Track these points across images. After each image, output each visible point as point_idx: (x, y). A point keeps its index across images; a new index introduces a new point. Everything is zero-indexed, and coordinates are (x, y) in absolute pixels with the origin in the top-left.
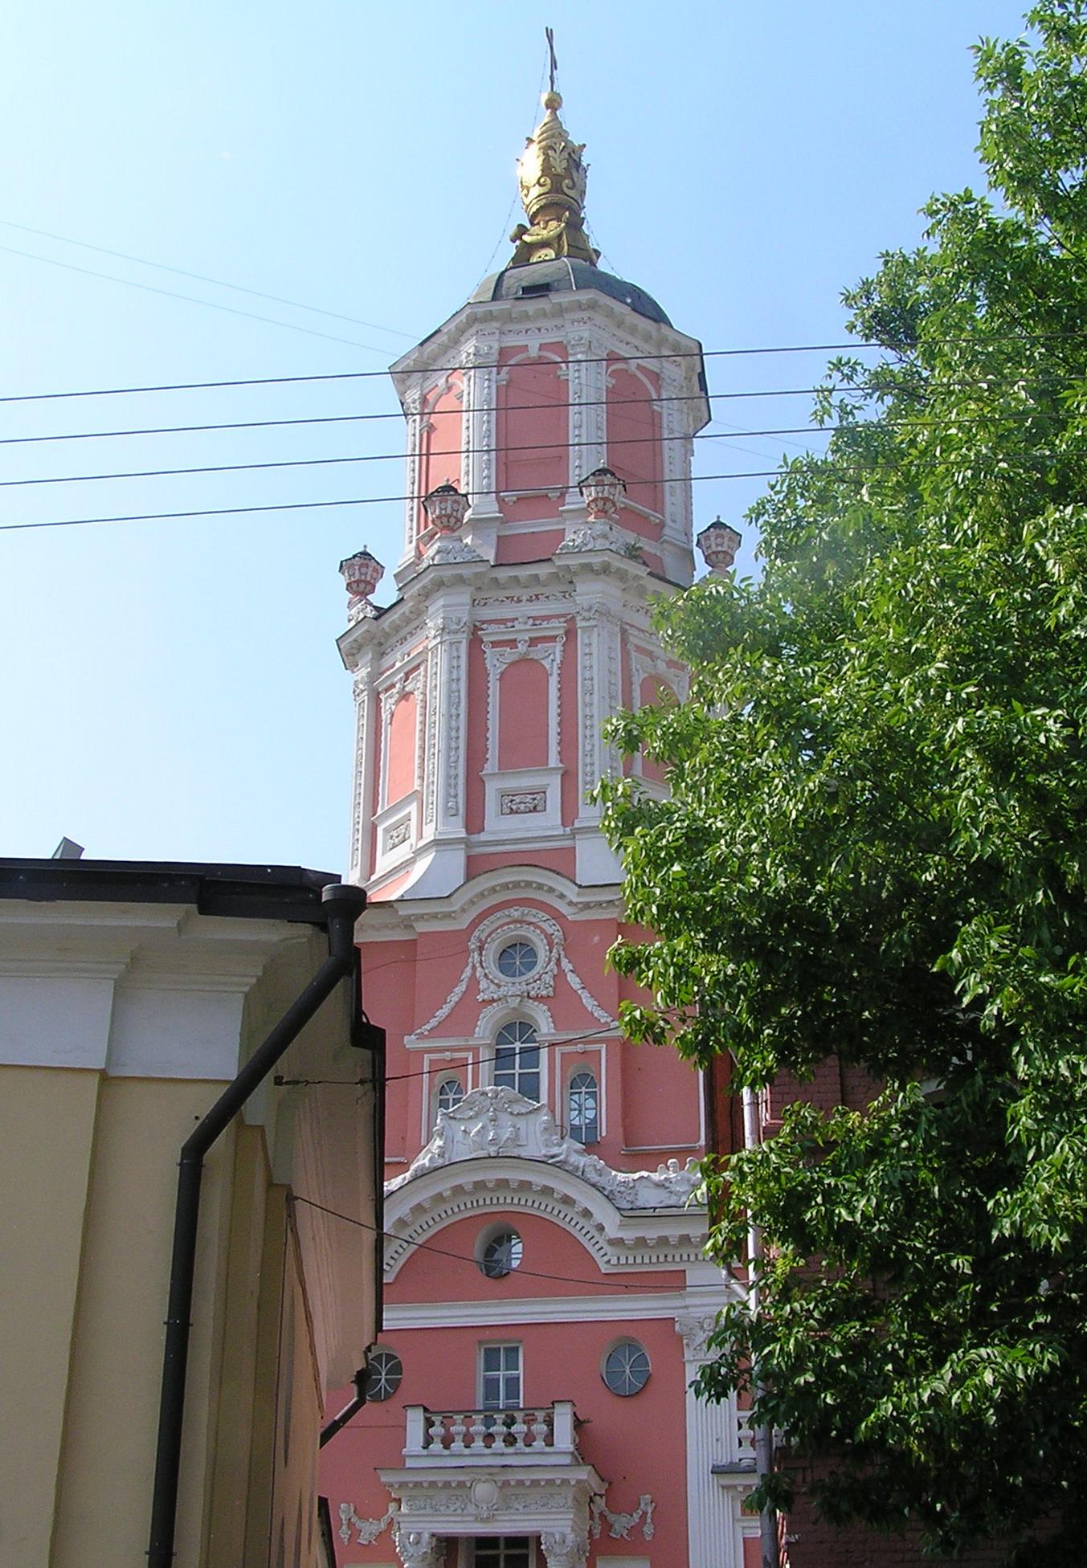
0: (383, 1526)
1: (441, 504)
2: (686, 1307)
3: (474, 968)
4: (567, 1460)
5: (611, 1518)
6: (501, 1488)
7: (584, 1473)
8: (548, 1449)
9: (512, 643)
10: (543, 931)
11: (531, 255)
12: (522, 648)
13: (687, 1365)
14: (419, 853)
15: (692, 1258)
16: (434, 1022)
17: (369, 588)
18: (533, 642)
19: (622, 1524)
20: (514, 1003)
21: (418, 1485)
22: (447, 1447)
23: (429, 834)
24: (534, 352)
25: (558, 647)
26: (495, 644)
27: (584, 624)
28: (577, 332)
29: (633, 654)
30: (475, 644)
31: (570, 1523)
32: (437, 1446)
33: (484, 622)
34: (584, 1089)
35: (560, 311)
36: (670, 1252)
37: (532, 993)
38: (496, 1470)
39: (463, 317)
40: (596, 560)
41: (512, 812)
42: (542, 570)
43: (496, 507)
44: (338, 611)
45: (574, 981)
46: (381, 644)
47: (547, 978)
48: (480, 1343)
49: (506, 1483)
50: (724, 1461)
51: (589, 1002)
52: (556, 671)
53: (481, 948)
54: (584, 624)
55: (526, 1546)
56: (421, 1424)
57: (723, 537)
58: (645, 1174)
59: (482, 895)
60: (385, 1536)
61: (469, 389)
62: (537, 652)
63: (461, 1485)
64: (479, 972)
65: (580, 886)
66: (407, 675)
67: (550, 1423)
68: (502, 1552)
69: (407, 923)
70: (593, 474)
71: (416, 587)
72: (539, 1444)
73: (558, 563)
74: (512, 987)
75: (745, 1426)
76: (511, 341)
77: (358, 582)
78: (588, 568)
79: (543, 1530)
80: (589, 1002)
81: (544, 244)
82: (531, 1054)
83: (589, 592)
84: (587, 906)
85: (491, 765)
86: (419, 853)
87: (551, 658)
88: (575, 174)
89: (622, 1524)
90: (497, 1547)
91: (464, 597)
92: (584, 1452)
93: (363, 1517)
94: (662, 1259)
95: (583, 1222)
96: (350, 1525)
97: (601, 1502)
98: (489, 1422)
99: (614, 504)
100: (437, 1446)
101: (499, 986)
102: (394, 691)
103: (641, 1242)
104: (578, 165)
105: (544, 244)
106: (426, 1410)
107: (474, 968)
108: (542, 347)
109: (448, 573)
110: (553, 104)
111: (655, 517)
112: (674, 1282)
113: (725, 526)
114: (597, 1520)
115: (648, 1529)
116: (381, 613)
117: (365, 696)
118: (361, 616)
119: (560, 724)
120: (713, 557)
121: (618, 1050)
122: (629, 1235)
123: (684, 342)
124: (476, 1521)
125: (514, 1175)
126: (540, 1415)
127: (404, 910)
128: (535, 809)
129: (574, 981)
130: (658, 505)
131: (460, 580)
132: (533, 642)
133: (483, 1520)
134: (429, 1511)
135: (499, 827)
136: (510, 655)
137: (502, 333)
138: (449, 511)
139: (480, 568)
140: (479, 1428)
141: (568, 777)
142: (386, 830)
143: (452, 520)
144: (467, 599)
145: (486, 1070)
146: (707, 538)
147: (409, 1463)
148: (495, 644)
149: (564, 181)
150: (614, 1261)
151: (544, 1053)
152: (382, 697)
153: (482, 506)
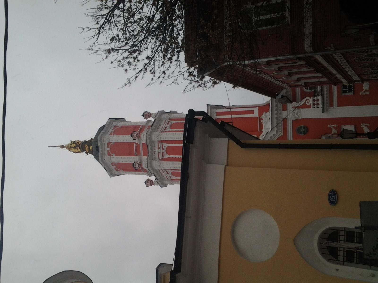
5: (333, 133)
9: (163, 153)
11: (91, 151)
12: (164, 151)
17: (151, 181)
18: (163, 149)
24: (109, 149)
25: (164, 144)
26: (163, 156)
27: (160, 139)
28: (106, 141)
29: (166, 130)
30: (163, 160)
33: (159, 158)
35: (101, 144)
42: (149, 147)
44: (156, 188)
46: (162, 179)
54: (160, 139)
57: (145, 114)
58: (263, 127)
62: (165, 148)
70: (132, 137)
71: (152, 171)
76: (106, 153)
77: (150, 183)
78: (150, 139)
81: (89, 148)
87: (166, 145)
88: (76, 142)
89: (334, 131)
97: (330, 135)
99: (138, 133)
102: (171, 176)
104: (75, 142)
105: (89, 148)
108: (108, 147)
110: (62, 147)
112: (285, 121)
113: (143, 114)
114: (333, 136)
115: (335, 126)
116: (156, 179)
118: (157, 182)
120: (149, 116)
130: (138, 127)
131: (151, 163)
132: (163, 149)
136: (165, 153)
138: (137, 164)
139: (149, 158)
143: (139, 164)
148: (163, 156)
149: (78, 147)
150: (281, 132)
152: (172, 178)
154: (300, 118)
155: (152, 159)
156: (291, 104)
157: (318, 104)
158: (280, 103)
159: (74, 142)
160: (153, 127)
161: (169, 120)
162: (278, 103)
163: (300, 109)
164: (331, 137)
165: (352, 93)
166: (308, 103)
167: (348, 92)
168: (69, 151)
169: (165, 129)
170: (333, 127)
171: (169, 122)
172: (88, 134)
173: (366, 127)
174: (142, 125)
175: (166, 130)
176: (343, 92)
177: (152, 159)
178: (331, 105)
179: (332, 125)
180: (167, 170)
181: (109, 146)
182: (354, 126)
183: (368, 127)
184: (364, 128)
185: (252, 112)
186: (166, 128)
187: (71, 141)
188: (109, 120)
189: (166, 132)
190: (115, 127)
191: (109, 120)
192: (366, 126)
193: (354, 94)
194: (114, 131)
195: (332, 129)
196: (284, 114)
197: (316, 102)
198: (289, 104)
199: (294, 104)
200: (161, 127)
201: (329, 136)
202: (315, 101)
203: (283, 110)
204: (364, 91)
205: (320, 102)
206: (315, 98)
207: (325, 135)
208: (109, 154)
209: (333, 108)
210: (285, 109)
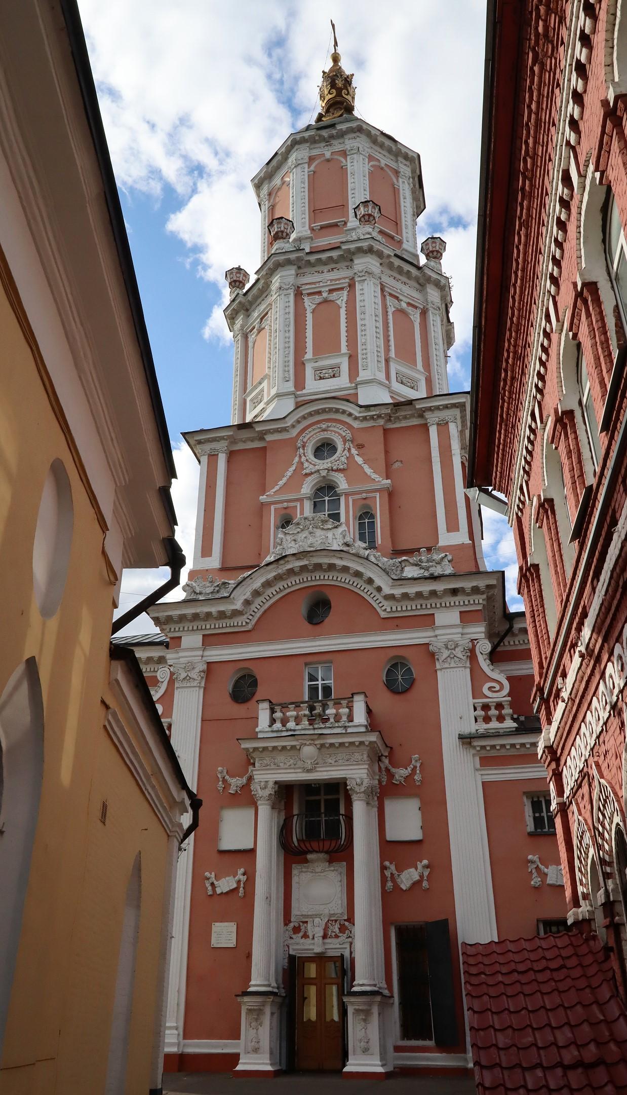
0: (244, 780)
1: (277, 229)
2: (436, 636)
3: (300, 457)
4: (363, 729)
5: (393, 770)
6: (319, 749)
7: (373, 737)
8: (351, 724)
9: (320, 293)
10: (340, 434)
12: (325, 295)
13: (438, 672)
14: (268, 403)
15: (438, 605)
16: (277, 488)
18: (331, 291)
19: (401, 773)
20: (324, 473)
21: (265, 749)
22: (284, 726)
23: (274, 392)
24: (328, 155)
25: (345, 293)
26: (309, 294)
29: (388, 297)
30: (299, 294)
31: (366, 771)
32: (278, 725)
34: (367, 521)
36: (423, 602)
38: (316, 737)
39: (289, 143)
40: (365, 245)
41: (321, 378)
43: (309, 232)
45: (359, 460)
47: (343, 459)
48: (306, 664)
49: (322, 745)
51: (368, 470)
52: (344, 305)
53: (304, 447)
55: (338, 792)
56: (268, 712)
59: (304, 418)
60: (246, 787)
61: (295, 180)
64: (303, 459)
65: (361, 407)
66: (262, 319)
67: (350, 708)
68: (323, 797)
69: (261, 436)
73: (344, 247)
74: (323, 465)
75: (479, 708)
78: (360, 250)
79: (348, 776)
80: (368, 470)
82: (335, 503)
83: (361, 263)
85: (309, 355)
86: (268, 403)
87: (342, 299)
90: (319, 794)
91: (291, 271)
92: (373, 725)
93: (232, 776)
94: (419, 607)
95: (368, 587)
96: (224, 781)
100: (278, 725)
101: (315, 465)
103: (405, 596)
106: (270, 702)
107: (300, 457)
109: (282, 258)
110: (336, 58)
111: (398, 237)
112: (428, 621)
114: (384, 773)
117: (239, 337)
121: (386, 495)
122: (398, 592)
123: (410, 154)
124: (303, 772)
125: (325, 561)
126: (344, 702)
127: (258, 428)
128: (334, 376)
129: (359, 460)
131: (289, 262)
132: (331, 291)
133: (309, 771)
134: (273, 766)
135: (313, 386)
137: (310, 149)
140: (307, 712)
141: (353, 359)
142: (251, 400)
144: (293, 272)
145: (308, 506)
146: (427, 244)
147: (260, 736)
148: (309, 294)
150: (389, 610)
153: (301, 229)
154: (438, 667)
155: (299, 268)
156: (483, 635)
158: (485, 603)
159: (348, 81)
162: (484, 596)
163: (468, 665)
165: (531, 827)
166: (490, 688)
167: (535, 818)
168: (323, 72)
169: (391, 295)
170: (412, 770)
171: (416, 307)
172: (373, 107)
173: (417, 878)
174: (405, 241)
175: (388, 297)
176: (535, 799)
177: (299, 268)
178: (487, 761)
181: (336, 157)
182: (417, 835)
183: (417, 884)
184: (412, 870)
185: (453, 526)
186: (397, 298)
187: (353, 75)
188: (415, 156)
189: (383, 296)
190: (397, 173)
191: (415, 156)
192: (422, 876)
193: (530, 834)
194: (382, 169)
196: (447, 617)
197: (493, 712)
198: (483, 629)
199: (485, 646)
200: (399, 285)
202: (496, 708)
203: (461, 612)
204: (542, 867)
205: (494, 724)
206: (507, 711)
207: (387, 746)
208: (311, 159)
209: (478, 766)
210: (466, 617)
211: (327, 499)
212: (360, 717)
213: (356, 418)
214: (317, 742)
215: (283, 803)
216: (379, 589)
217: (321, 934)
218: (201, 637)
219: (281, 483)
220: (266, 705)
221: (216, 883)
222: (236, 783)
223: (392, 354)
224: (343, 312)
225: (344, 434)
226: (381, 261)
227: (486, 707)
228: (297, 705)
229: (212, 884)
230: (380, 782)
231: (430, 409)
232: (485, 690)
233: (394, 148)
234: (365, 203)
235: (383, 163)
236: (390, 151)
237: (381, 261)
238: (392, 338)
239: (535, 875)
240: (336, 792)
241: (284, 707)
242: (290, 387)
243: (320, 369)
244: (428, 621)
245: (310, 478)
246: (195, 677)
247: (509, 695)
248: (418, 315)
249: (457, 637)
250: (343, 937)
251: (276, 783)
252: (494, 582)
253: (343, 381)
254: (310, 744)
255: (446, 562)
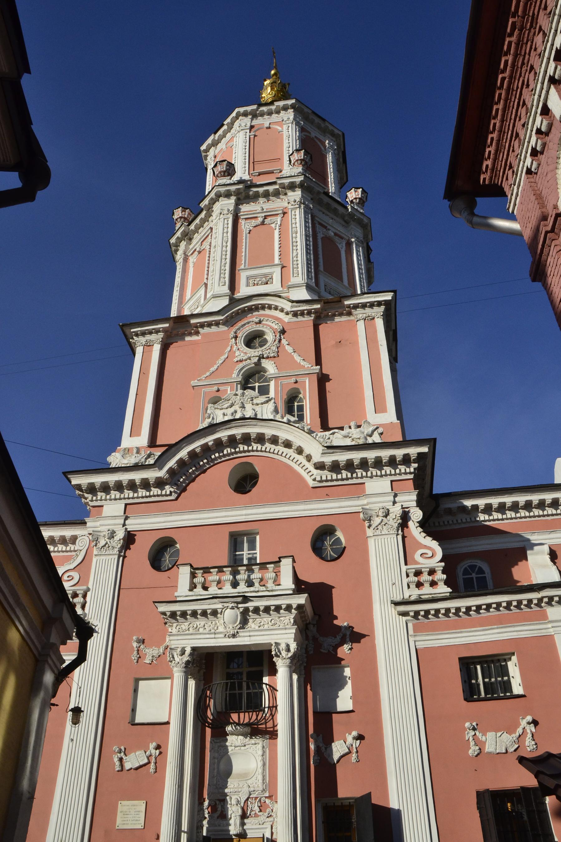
5: (321, 639)
8: (278, 587)
10: (271, 327)
16: (208, 374)
25: (279, 219)
29: (317, 225)
31: (293, 636)
32: (199, 590)
37: (265, 356)
45: (289, 349)
47: (274, 348)
50: (398, 598)
56: (188, 576)
63: (215, 613)
64: (235, 348)
65: (293, 302)
67: (277, 574)
72: (270, 585)
74: (254, 353)
75: (411, 575)
84: (295, 314)
92: (300, 586)
97: (313, 629)
98: (235, 573)
100: (199, 590)
106: (191, 566)
119: (280, 248)
122: (328, 459)
128: (267, 283)
129: (289, 349)
147: (178, 599)
148: (246, 219)
151: (272, 384)
156: (414, 504)
157: (419, 585)
160: (326, 199)
161: (347, 238)
164: (306, 634)
171: (342, 238)
175: (317, 225)
179: (348, 636)
180: (210, 236)
188: (340, 133)
191: (340, 133)
195: (336, 637)
197: (425, 577)
198: (415, 498)
201: (311, 627)
205: (427, 591)
206: (440, 576)
211: (257, 385)
212: (287, 583)
213: (287, 314)
214: (240, 606)
215: (202, 672)
216: (309, 458)
217: (240, 812)
218: (123, 506)
219: (212, 369)
220: (187, 569)
221: (124, 757)
222: (150, 653)
223: (321, 268)
224: (276, 233)
225: (276, 327)
226: (312, 196)
227: (418, 573)
228: (220, 569)
229: (121, 760)
230: (307, 652)
231: (356, 307)
232: (417, 557)
233: (323, 125)
234: (298, 151)
235: (313, 135)
236: (319, 127)
237: (312, 196)
238: (321, 256)
239: (472, 743)
240: (259, 660)
241: (206, 570)
242: (226, 289)
243: (254, 277)
244: (358, 490)
245: (241, 365)
246: (114, 544)
247: (441, 561)
248: (344, 245)
249: (389, 505)
250: (263, 817)
251: (194, 649)
252: (425, 449)
253: (275, 286)
254: (232, 608)
255: (376, 434)
